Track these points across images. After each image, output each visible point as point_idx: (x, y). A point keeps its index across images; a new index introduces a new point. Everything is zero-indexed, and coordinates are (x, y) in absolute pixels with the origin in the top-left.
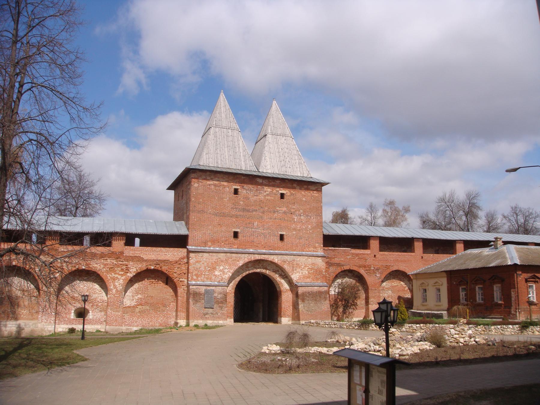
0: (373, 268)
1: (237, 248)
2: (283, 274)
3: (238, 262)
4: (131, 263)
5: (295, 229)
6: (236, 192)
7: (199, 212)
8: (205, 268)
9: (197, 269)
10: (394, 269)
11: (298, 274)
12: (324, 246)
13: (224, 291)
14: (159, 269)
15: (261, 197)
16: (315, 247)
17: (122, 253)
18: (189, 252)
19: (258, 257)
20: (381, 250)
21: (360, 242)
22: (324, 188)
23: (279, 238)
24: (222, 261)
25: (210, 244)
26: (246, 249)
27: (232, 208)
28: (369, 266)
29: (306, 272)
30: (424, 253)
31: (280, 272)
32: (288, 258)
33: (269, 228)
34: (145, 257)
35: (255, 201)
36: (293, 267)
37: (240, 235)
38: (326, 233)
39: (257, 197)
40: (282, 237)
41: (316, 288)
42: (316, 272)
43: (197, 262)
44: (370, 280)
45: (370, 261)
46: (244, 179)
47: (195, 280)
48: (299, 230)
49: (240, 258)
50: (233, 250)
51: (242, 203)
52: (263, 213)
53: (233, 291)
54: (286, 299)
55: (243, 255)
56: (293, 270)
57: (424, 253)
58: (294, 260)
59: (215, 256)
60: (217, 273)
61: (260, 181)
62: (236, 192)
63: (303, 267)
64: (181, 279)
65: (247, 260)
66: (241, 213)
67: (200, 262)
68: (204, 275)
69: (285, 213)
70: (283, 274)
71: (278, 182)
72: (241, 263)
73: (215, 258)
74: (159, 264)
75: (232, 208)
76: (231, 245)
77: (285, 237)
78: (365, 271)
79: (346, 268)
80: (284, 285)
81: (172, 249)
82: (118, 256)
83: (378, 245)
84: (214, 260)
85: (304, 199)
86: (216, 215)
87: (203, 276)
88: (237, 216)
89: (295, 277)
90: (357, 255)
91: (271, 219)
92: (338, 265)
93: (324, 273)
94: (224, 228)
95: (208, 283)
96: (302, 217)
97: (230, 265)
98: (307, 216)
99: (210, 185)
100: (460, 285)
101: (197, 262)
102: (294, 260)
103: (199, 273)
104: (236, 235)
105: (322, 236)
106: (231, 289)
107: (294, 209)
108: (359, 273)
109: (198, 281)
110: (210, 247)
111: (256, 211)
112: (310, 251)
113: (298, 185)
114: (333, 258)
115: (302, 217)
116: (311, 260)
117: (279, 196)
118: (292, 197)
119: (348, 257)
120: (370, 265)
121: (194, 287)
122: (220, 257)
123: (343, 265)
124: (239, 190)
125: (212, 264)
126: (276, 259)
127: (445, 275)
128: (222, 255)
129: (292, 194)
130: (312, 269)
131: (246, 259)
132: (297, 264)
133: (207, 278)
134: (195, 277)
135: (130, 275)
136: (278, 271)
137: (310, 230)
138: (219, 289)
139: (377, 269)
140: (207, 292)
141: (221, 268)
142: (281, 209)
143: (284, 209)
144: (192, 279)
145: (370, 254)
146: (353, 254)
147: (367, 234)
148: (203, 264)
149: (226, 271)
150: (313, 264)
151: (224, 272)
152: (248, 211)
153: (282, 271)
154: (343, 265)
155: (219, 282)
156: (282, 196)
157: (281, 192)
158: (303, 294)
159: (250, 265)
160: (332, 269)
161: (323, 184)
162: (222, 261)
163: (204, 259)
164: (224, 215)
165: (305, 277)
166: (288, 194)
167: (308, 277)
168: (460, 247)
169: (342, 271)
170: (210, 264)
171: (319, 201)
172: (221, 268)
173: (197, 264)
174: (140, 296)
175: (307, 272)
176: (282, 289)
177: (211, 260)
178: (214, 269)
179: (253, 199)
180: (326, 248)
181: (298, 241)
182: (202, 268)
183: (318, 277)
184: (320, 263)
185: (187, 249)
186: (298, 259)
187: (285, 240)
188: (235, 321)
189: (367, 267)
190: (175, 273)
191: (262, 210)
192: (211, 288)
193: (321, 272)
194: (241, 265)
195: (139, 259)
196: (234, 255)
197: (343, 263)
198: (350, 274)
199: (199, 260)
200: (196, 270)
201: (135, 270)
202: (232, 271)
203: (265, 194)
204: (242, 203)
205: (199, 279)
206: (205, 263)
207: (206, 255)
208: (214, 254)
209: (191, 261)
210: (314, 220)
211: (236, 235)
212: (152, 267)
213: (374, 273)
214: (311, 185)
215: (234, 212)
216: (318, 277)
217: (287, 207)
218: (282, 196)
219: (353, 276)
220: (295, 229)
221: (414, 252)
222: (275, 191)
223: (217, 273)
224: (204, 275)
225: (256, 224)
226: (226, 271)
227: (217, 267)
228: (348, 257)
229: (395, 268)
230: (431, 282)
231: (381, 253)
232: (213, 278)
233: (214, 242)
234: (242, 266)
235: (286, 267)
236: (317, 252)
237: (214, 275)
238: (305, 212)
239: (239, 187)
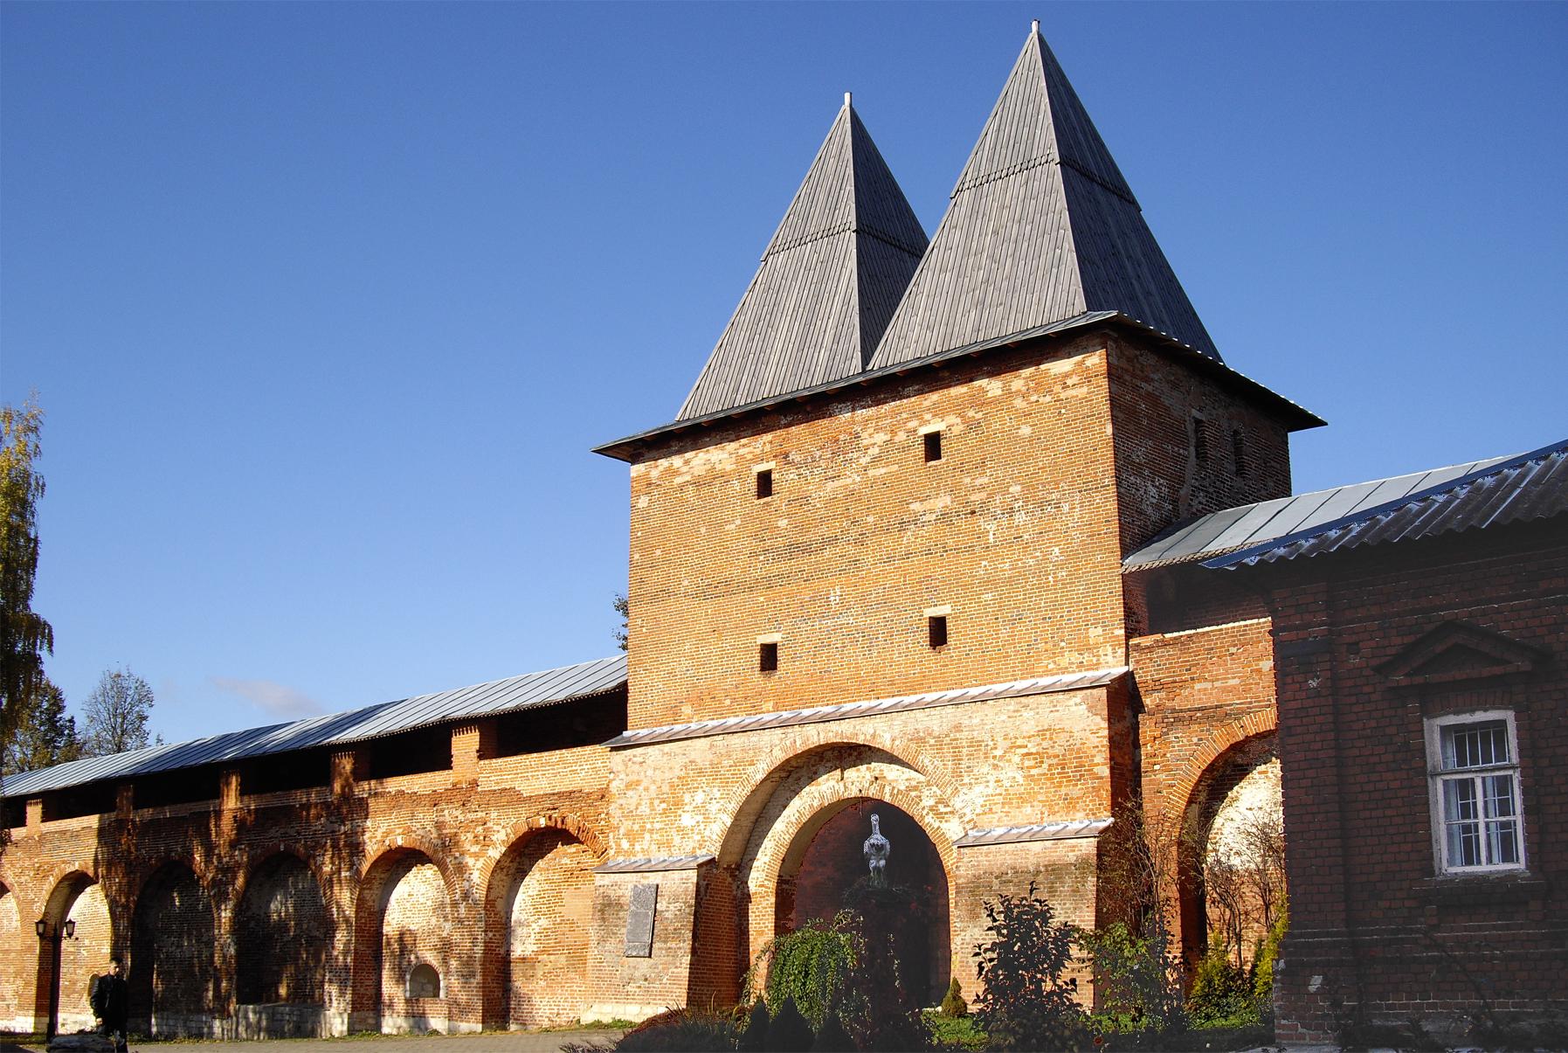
3: (750, 769)
4: (494, 815)
5: (989, 583)
6: (765, 484)
7: (654, 598)
9: (629, 815)
11: (978, 789)
15: (852, 479)
17: (474, 784)
24: (701, 772)
25: (687, 710)
27: (754, 554)
34: (526, 789)
36: (957, 760)
39: (837, 483)
40: (938, 632)
43: (629, 786)
52: (860, 542)
56: (958, 775)
58: (958, 728)
60: (687, 820)
62: (765, 484)
65: (780, 756)
66: (783, 567)
67: (638, 783)
68: (651, 831)
69: (944, 517)
72: (759, 772)
73: (681, 760)
75: (754, 554)
77: (950, 625)
81: (588, 749)
82: (466, 794)
84: (678, 773)
86: (703, 594)
87: (647, 836)
91: (890, 559)
97: (725, 783)
98: (1041, 506)
99: (681, 487)
101: (629, 786)
102: (958, 728)
104: (769, 658)
107: (982, 488)
112: (1064, 670)
115: (1020, 518)
116: (1034, 716)
117: (920, 450)
118: (972, 439)
121: (608, 879)
123: (1238, 715)
129: (972, 426)
130: (1039, 758)
132: (975, 744)
134: (625, 845)
135: (496, 853)
140: (638, 894)
141: (700, 797)
142: (927, 505)
143: (943, 502)
149: (714, 807)
150: (1042, 733)
152: (806, 549)
154: (1238, 715)
156: (933, 446)
165: (1012, 800)
166: (956, 430)
170: (666, 788)
173: (630, 793)
174: (544, 922)
177: (668, 775)
178: (678, 804)
182: (645, 809)
183: (1076, 792)
187: (951, 640)
191: (854, 533)
194: (760, 777)
195: (508, 797)
196: (736, 740)
197: (1236, 701)
199: (635, 778)
201: (502, 836)
202: (733, 806)
203: (863, 461)
204: (783, 523)
206: (653, 787)
211: (769, 658)
212: (543, 822)
215: (759, 570)
216: (1076, 792)
220: (989, 583)
222: (901, 436)
224: (651, 831)
226: (714, 807)
227: (687, 798)
236: (1096, 666)
238: (1027, 488)
239: (771, 465)
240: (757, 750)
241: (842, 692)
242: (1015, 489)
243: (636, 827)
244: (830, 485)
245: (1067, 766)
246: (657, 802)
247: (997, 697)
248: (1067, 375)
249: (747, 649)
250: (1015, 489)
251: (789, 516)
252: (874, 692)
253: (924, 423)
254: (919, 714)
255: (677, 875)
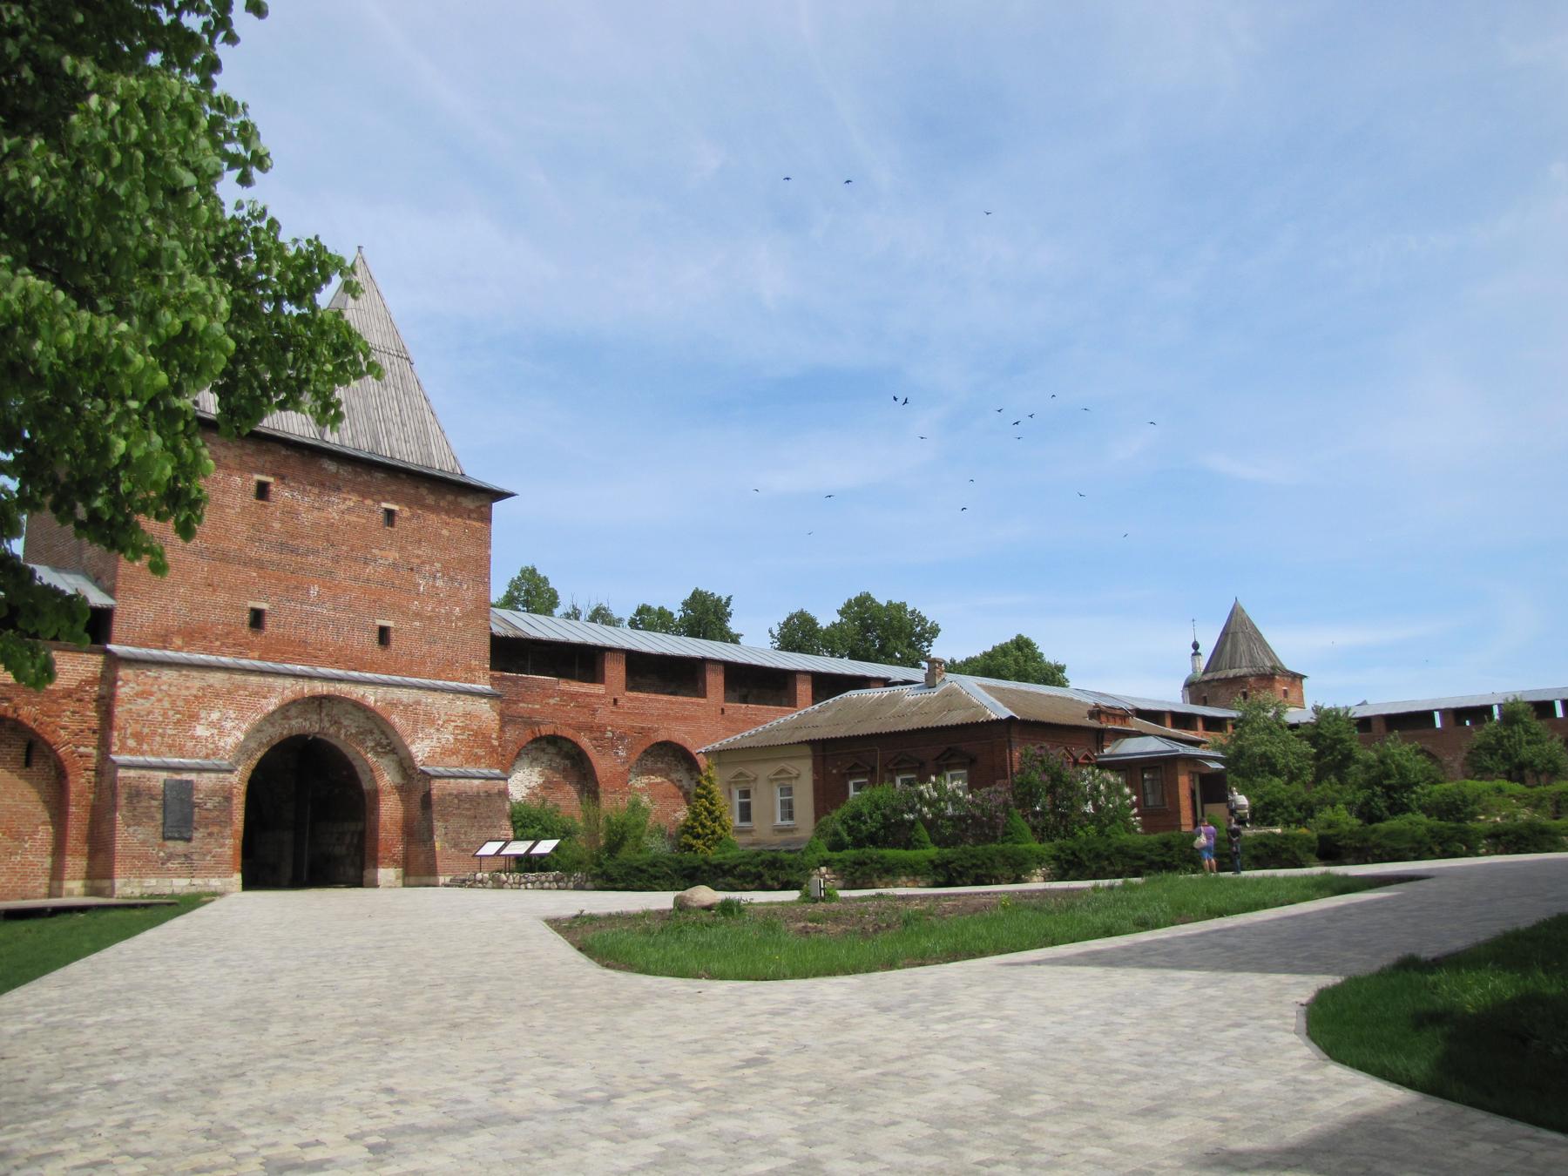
0: (609, 735)
1: (260, 659)
2: (385, 742)
3: (264, 701)
5: (418, 615)
6: (262, 491)
8: (165, 715)
9: (137, 717)
10: (660, 739)
11: (427, 742)
12: (492, 668)
13: (222, 788)
14: (10, 713)
15: (333, 514)
16: (469, 669)
18: (114, 661)
19: (321, 688)
20: (630, 688)
21: (579, 661)
22: (497, 506)
23: (376, 635)
26: (284, 662)
28: (601, 729)
29: (448, 737)
30: (727, 700)
31: (377, 735)
32: (405, 695)
33: (350, 606)
35: (315, 525)
36: (416, 722)
37: (269, 622)
38: (498, 630)
41: (476, 782)
42: (475, 742)
43: (140, 695)
44: (603, 765)
45: (604, 715)
46: (287, 457)
47: (132, 751)
48: (430, 618)
49: (271, 689)
50: (245, 662)
51: (277, 525)
52: (336, 560)
53: (243, 788)
54: (390, 810)
55: (279, 682)
57: (727, 700)
59: (196, 681)
60: (201, 731)
61: (331, 467)
62: (262, 491)
63: (440, 723)
64: (82, 749)
65: (289, 695)
66: (275, 557)
68: (162, 736)
69: (395, 565)
70: (385, 742)
71: (380, 476)
72: (272, 704)
73: (197, 684)
74: (9, 700)
75: (251, 539)
76: (241, 648)
77: (393, 635)
78: (591, 739)
79: (546, 730)
80: (386, 777)
83: (623, 674)
85: (445, 532)
88: (260, 565)
89: (421, 749)
90: (573, 696)
91: (356, 579)
92: (529, 722)
93: (496, 743)
94: (222, 598)
95: (176, 761)
96: (439, 583)
97: (241, 709)
98: (452, 579)
100: (852, 776)
101: (140, 695)
102: (418, 703)
103: (146, 730)
104: (257, 619)
105: (488, 640)
106: (237, 781)
107: (418, 557)
108: (575, 745)
109: (143, 754)
110: (179, 649)
111: (316, 552)
113: (431, 491)
114: (516, 702)
115: (439, 583)
116: (461, 705)
119: (552, 701)
120: (605, 726)
121: (132, 773)
122: (211, 681)
124: (273, 488)
125: (186, 701)
126: (371, 696)
127: (808, 750)
128: (217, 679)
130: (463, 728)
131: (289, 689)
133: (170, 747)
134: (131, 743)
136: (371, 732)
137: (458, 619)
138: (206, 781)
139: (621, 738)
141: (215, 716)
143: (393, 555)
144: (124, 748)
145: (604, 696)
146: (563, 693)
147: (599, 643)
148: (160, 700)
149: (229, 725)
150: (466, 715)
151: (221, 732)
153: (383, 732)
154: (538, 724)
155: (207, 757)
157: (385, 505)
158: (442, 799)
159: (293, 712)
160: (511, 733)
161: (500, 495)
162: (217, 696)
163: (164, 687)
164: (225, 558)
165: (447, 752)
167: (454, 752)
168: (804, 689)
169: (535, 740)
171: (485, 542)
172: (215, 716)
173: (140, 701)
175: (451, 738)
176: (381, 784)
177: (185, 692)
178: (194, 717)
179: (307, 518)
180: (497, 674)
181: (425, 648)
183: (481, 752)
184: (486, 712)
185: (107, 652)
186: (429, 698)
187: (393, 644)
188: (250, 883)
189: (595, 730)
190: (68, 730)
191: (331, 553)
192: (185, 776)
193: (486, 738)
194: (271, 708)
196: (253, 679)
197: (537, 718)
198: (551, 750)
200: (137, 722)
204: (277, 525)
205: (145, 747)
207: (168, 675)
208: (194, 674)
209: (123, 691)
210: (468, 593)
211: (257, 619)
213: (614, 746)
214: (465, 495)
216: (481, 752)
217: (402, 549)
218: (390, 514)
219: (558, 754)
220: (418, 615)
221: (704, 696)
223: (201, 731)
224: (162, 736)
225: (314, 591)
226: (229, 725)
227: (203, 714)
228: (553, 699)
229: (662, 736)
230: (765, 771)
231: (634, 694)
232: (190, 744)
233: (192, 635)
234: (274, 712)
235: (396, 719)
237: (193, 737)
238: (445, 568)
239: (271, 480)
240: (271, 689)
241: (311, 658)
242: (438, 565)
243: (146, 730)
244: (316, 513)
245: (480, 737)
246: (171, 713)
247: (443, 690)
248: (471, 511)
249: (238, 609)
250: (438, 565)
251: (283, 522)
252: (335, 663)
253: (386, 501)
254: (396, 690)
255: (213, 775)
